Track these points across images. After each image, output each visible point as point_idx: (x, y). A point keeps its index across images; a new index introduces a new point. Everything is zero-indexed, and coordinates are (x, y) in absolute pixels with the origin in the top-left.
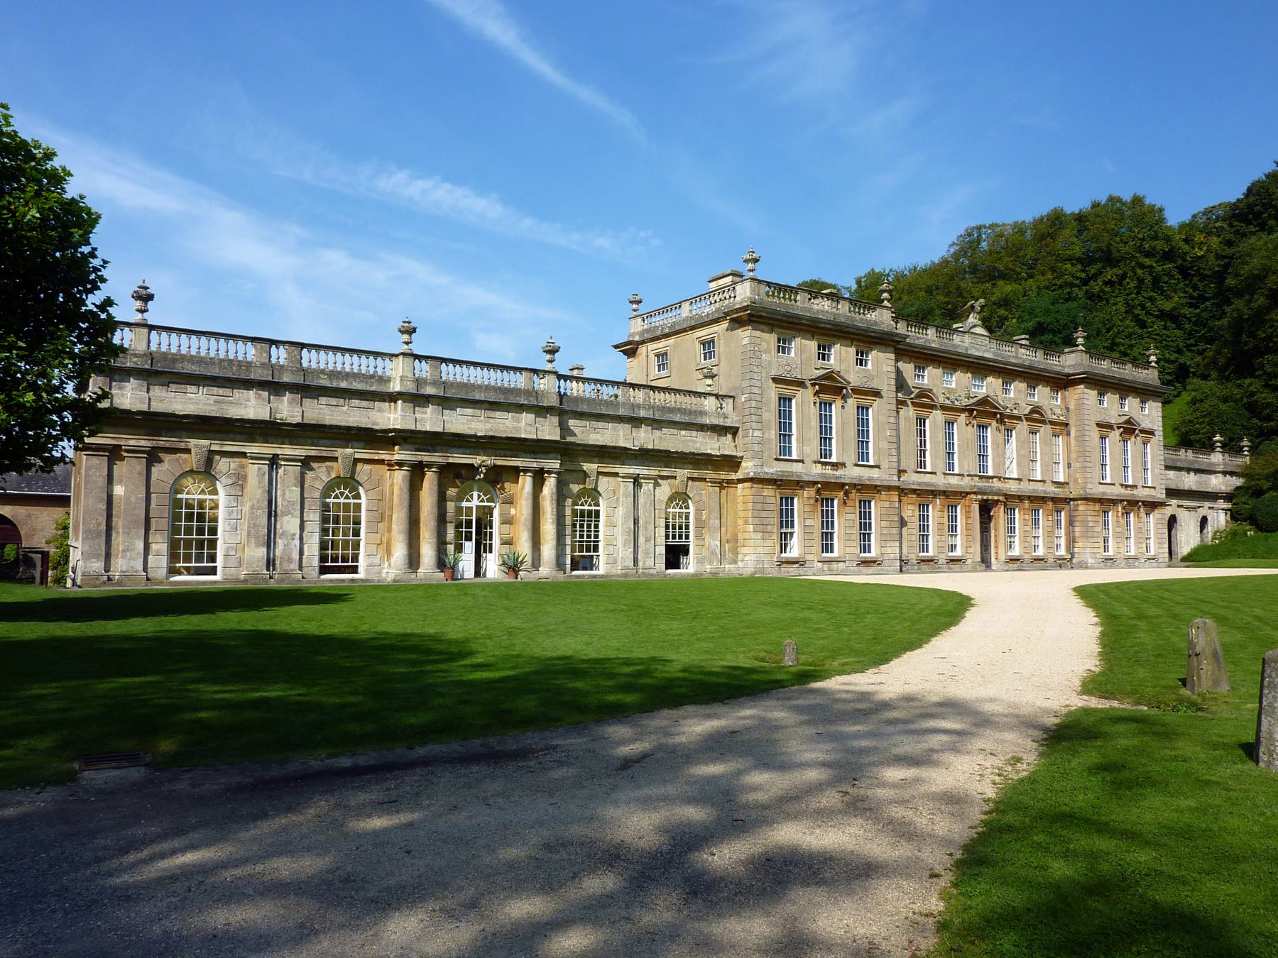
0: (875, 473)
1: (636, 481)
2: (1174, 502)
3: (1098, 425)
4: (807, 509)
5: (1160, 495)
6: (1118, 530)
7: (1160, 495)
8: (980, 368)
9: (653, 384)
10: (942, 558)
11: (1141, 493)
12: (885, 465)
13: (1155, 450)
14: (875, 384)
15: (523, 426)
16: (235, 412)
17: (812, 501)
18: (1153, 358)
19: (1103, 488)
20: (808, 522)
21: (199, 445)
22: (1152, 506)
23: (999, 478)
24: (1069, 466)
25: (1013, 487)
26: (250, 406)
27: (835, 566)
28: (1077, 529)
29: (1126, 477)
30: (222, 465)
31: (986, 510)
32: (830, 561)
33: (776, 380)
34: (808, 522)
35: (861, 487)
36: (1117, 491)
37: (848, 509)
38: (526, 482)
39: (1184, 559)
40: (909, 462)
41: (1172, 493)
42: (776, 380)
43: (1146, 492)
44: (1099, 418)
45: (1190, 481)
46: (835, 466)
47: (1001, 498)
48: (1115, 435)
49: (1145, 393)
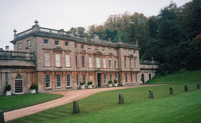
1: (6, 73)
2: (143, 71)
3: (124, 56)
4: (53, 77)
5: (139, 70)
6: (129, 78)
7: (139, 70)
8: (97, 45)
9: (19, 51)
11: (134, 70)
12: (73, 67)
13: (138, 60)
14: (70, 49)
17: (54, 76)
18: (137, 42)
19: (125, 69)
20: (53, 80)
22: (137, 72)
23: (102, 68)
24: (118, 65)
27: (61, 89)
28: (120, 78)
29: (131, 67)
31: (99, 75)
32: (59, 88)
33: (43, 49)
34: (53, 80)
35: (66, 72)
36: (128, 70)
37: (63, 77)
39: (146, 83)
40: (80, 65)
41: (141, 69)
42: (43, 49)
43: (136, 70)
45: (147, 67)
47: (102, 72)
48: (128, 58)
49: (135, 49)
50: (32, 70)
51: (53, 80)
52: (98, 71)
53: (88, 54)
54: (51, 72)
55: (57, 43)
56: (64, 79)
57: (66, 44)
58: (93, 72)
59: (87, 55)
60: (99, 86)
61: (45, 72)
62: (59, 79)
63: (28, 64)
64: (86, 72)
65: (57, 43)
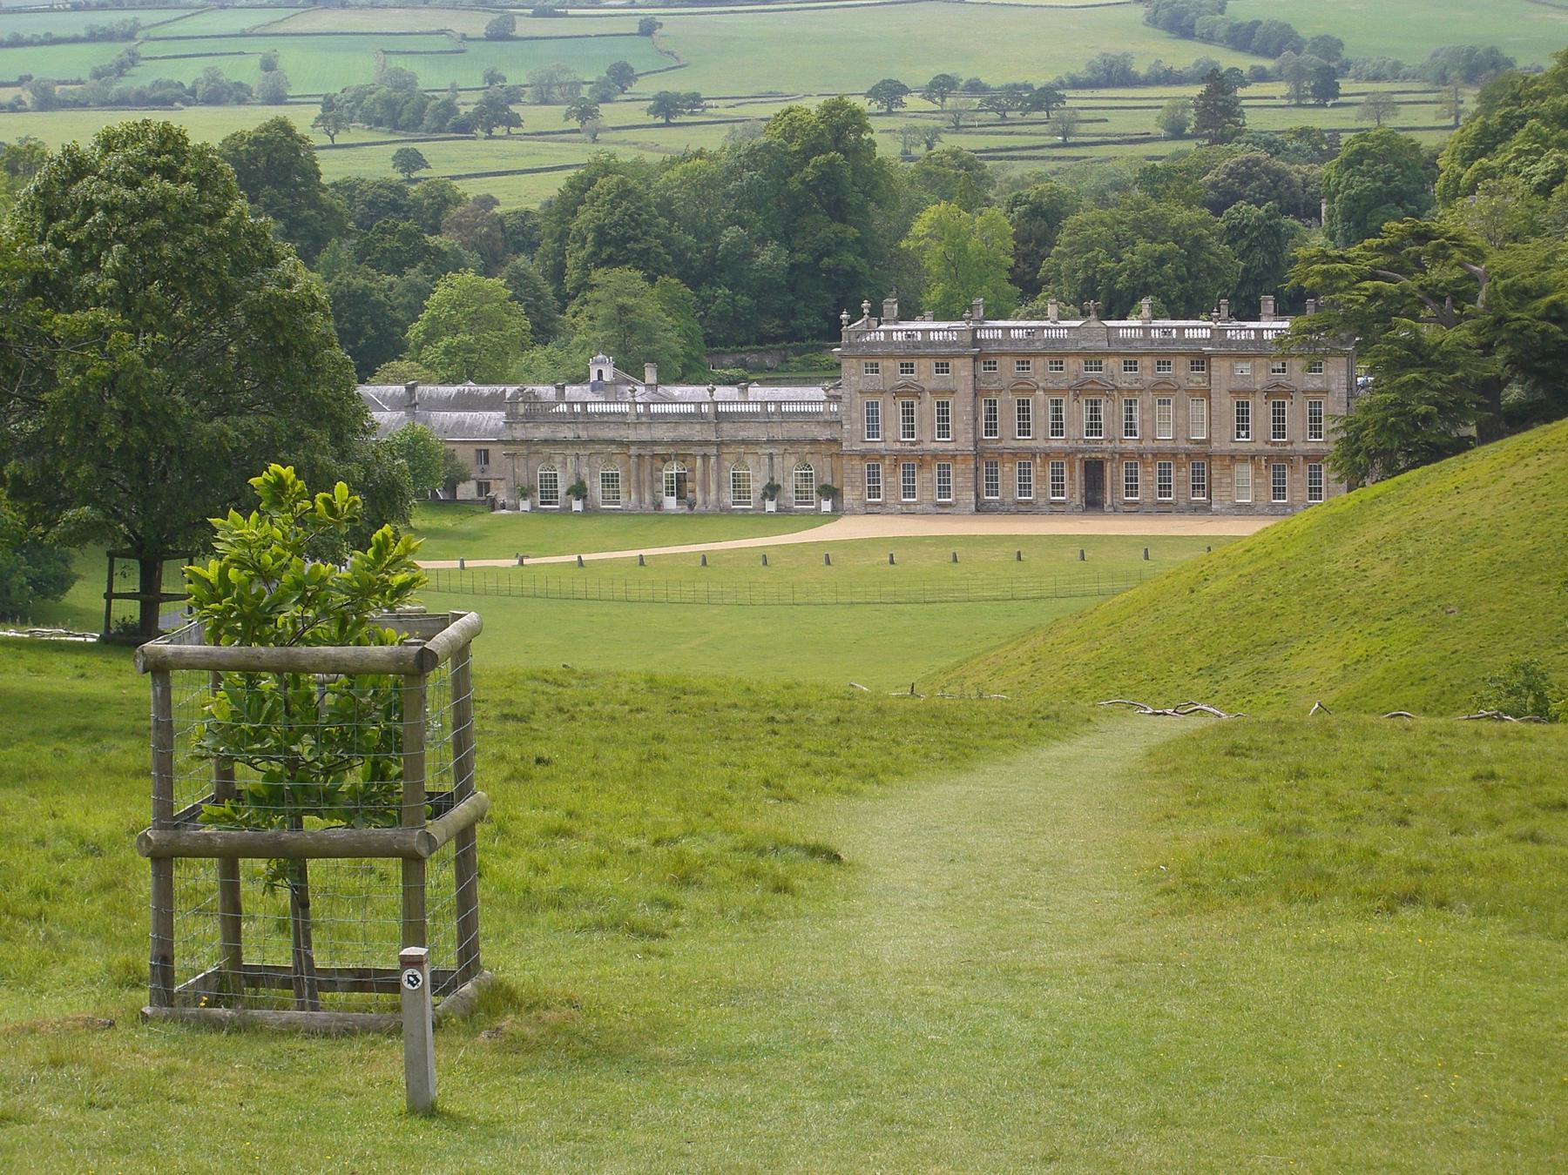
0: (951, 446)
1: (771, 456)
10: (1042, 501)
12: (961, 439)
15: (696, 432)
16: (560, 436)
21: (547, 450)
25: (1130, 444)
26: (567, 433)
30: (558, 459)
32: (908, 504)
35: (935, 456)
36: (1260, 446)
38: (699, 461)
44: (1233, 385)
46: (912, 444)
50: (834, 449)
51: (891, 480)
52: (1084, 451)
53: (1045, 390)
54: (883, 457)
55: (907, 368)
56: (926, 479)
57: (942, 368)
58: (1067, 455)
59: (1040, 393)
60: (1093, 502)
61: (863, 456)
62: (909, 477)
63: (825, 434)
64: (1034, 455)
65: (907, 368)
